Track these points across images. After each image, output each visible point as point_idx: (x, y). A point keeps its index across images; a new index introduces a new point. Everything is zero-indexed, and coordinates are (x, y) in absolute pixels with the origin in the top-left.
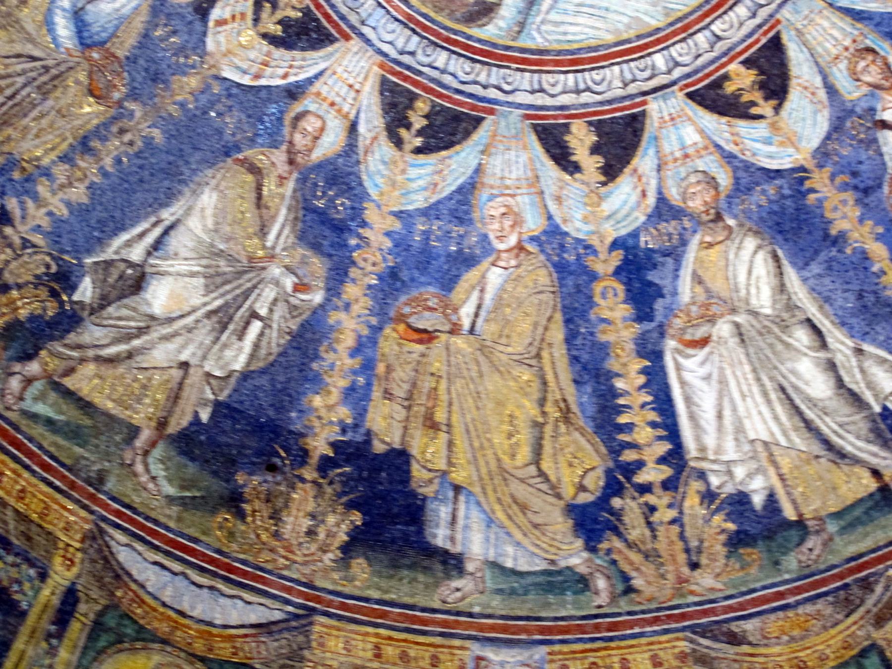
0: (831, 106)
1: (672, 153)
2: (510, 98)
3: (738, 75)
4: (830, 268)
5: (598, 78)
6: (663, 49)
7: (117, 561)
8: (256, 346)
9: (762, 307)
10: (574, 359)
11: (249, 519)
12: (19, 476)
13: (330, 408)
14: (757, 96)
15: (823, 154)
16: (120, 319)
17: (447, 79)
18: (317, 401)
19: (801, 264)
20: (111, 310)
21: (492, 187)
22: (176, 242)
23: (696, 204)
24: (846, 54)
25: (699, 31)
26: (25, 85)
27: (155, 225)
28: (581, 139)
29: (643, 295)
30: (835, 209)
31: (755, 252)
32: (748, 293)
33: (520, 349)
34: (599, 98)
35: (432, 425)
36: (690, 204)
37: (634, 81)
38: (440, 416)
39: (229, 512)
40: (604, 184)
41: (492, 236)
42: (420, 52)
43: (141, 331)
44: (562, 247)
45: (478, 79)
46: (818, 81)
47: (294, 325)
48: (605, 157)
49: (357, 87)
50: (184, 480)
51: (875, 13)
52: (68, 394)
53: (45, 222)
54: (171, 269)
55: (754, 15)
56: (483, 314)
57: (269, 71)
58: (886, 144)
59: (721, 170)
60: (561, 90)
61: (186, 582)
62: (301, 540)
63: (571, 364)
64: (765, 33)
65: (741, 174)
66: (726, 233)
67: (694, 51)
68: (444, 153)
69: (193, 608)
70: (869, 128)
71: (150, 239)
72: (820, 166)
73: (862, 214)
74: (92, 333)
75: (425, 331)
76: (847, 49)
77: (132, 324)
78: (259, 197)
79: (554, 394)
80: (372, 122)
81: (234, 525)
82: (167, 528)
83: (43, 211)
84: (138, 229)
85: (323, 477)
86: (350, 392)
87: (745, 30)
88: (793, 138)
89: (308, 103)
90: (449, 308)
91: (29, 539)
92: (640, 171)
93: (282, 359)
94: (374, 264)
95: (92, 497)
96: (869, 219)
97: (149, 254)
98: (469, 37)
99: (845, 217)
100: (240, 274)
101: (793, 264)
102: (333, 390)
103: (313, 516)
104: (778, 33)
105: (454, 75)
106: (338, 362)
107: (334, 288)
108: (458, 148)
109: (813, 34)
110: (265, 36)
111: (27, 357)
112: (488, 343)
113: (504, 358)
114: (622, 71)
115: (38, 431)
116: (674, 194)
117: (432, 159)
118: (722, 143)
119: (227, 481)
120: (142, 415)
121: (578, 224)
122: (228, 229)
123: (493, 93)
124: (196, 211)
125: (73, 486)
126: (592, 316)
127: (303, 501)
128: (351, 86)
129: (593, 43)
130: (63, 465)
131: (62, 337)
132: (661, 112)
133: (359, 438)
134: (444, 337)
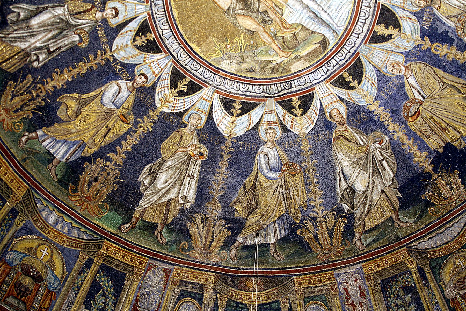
2: (357, 46)
7: (421, 249)
8: (389, 166)
10: (452, 73)
11: (436, 204)
12: (382, 259)
13: (421, 157)
16: (359, 202)
17: (341, 63)
18: (416, 159)
20: (355, 203)
21: (382, 66)
22: (347, 173)
26: (283, 194)
27: (339, 176)
28: (381, 30)
29: (444, 38)
32: (463, 4)
33: (439, 87)
35: (444, 130)
36: (421, 6)
37: (370, 3)
38: (444, 125)
39: (430, 207)
40: (400, 29)
41: (398, 74)
42: (328, 68)
43: (366, 198)
44: (414, 54)
47: (390, 151)
49: (330, 93)
50: (413, 214)
52: (369, 231)
53: (322, 208)
54: (354, 179)
56: (421, 91)
57: (312, 118)
60: (362, 29)
61: (440, 235)
62: (451, 193)
63: (453, 75)
68: (364, 76)
69: (447, 239)
71: (342, 179)
74: (358, 213)
75: (416, 112)
77: (362, 199)
78: (348, 140)
79: (459, 86)
80: (343, 93)
81: (434, 209)
82: (422, 229)
83: (318, 206)
84: (338, 181)
85: (438, 174)
86: (419, 149)
89: (327, 111)
90: (413, 101)
91: (398, 269)
92: (402, 16)
93: (398, 161)
94: (386, 116)
95: (401, 243)
97: (346, 182)
98: (331, 50)
100: (367, 159)
102: (415, 152)
103: (448, 184)
106: (409, 145)
107: (387, 133)
108: (364, 70)
110: (302, 115)
111: (354, 235)
112: (431, 96)
113: (439, 93)
115: (374, 246)
116: (415, 9)
117: (364, 80)
119: (421, 202)
120: (388, 213)
121: (409, 45)
122: (352, 154)
123: (352, 51)
124: (342, 161)
125: (394, 246)
126: (442, 58)
127: (441, 183)
128: (329, 95)
129: (351, 11)
130: (387, 245)
131: (354, 223)
133: (435, 154)
134: (421, 108)
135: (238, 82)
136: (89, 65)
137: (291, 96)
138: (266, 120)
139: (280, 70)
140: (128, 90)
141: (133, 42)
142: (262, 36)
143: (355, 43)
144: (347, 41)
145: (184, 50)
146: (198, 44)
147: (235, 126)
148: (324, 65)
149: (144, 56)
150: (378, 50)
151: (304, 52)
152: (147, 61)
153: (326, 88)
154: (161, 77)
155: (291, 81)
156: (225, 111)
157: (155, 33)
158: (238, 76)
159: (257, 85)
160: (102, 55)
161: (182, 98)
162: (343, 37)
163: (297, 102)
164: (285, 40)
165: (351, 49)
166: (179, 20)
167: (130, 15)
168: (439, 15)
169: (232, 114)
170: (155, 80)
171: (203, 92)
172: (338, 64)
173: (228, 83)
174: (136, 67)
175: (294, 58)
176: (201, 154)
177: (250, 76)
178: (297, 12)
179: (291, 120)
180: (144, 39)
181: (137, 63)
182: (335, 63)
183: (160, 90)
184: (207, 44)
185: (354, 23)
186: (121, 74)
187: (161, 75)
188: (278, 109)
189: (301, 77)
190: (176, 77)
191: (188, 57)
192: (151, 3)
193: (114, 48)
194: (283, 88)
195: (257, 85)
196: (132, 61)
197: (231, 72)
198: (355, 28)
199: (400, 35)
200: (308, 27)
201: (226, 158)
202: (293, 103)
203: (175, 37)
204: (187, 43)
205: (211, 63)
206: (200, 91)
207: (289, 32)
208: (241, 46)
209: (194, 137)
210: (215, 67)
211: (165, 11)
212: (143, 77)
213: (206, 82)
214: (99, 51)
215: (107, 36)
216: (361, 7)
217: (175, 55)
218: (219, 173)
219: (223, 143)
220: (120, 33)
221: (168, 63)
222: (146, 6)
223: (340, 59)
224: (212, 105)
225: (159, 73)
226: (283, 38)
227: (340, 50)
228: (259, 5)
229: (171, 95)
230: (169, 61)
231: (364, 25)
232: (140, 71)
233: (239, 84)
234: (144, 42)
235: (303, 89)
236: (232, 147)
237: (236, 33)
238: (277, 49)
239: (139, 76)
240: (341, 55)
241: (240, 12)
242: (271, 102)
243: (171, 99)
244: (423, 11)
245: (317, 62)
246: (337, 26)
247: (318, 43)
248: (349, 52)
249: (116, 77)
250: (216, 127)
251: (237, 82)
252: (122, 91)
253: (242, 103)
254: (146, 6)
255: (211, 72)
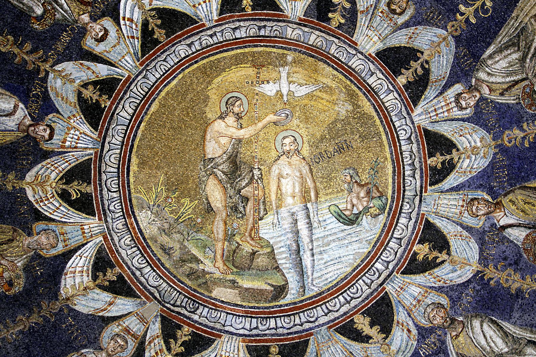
0: (473, 235)
1: (411, 304)
2: (317, 324)
3: (420, 250)
4: (523, 310)
5: (354, 291)
6: (377, 259)
9: (502, 349)
14: (435, 253)
15: (483, 259)
17: (280, 331)
19: (508, 317)
23: (438, 321)
24: (464, 208)
25: (389, 241)
28: (362, 323)
30: (507, 280)
31: (482, 326)
32: (491, 347)
34: (360, 299)
37: (373, 282)
42: (259, 325)
45: (296, 323)
46: (459, 228)
48: (379, 325)
51: (464, 182)
55: (410, 219)
58: (510, 236)
59: (440, 298)
60: (339, 307)
64: (421, 224)
65: (451, 293)
66: (461, 325)
67: (392, 251)
70: (498, 234)
72: (486, 266)
73: (522, 274)
76: (463, 206)
87: (410, 229)
88: (465, 262)
92: (401, 321)
96: (526, 275)
98: (281, 306)
99: (514, 281)
101: (504, 319)
104: (426, 219)
105: (283, 327)
109: (442, 210)
114: (363, 281)
116: (423, 322)
118: (434, 285)
123: (307, 326)
129: (342, 276)
132: (394, 288)
135: (139, 249)
136: (16, 51)
137: (184, 322)
138: (127, 323)
139: (201, 281)
140: (19, 124)
141: (82, 86)
142: (216, 223)
143: (317, 319)
144: (310, 309)
145: (120, 154)
146: (142, 164)
147: (84, 295)
148: (257, 318)
149: (75, 113)
150: (339, 346)
151: (246, 283)
152: (72, 121)
153: (236, 348)
154: (67, 154)
155: (202, 305)
156: (90, 267)
157: (112, 103)
158: (147, 243)
159: (157, 274)
160: (39, 58)
161: (61, 202)
162: (308, 302)
163: (185, 335)
164: (237, 251)
165: (306, 322)
166: (150, 118)
167: (112, 56)
168: (450, 347)
169: (95, 278)
170: (56, 150)
171: (91, 221)
172: (276, 329)
173: (127, 240)
174: (55, 114)
175: (230, 280)
176: (10, 284)
177: (159, 256)
178: (279, 229)
179: (157, 348)
180: (95, 97)
181: (60, 110)
182: (273, 325)
183: (49, 166)
184: (150, 174)
185: (336, 292)
186: (33, 102)
187: (67, 152)
188: (154, 324)
189: (216, 310)
190: (81, 172)
191: (117, 166)
192: (143, 70)
193: (58, 67)
194: (184, 304)
195: (157, 274)
196: (58, 103)
197: (144, 231)
198: (331, 300)
199: (382, 345)
200: (277, 257)
201: (35, 319)
202: (179, 333)
203: (126, 131)
204: (131, 152)
205: (133, 199)
206: (88, 216)
207: (251, 245)
208: (183, 213)
209: (25, 256)
210: (132, 208)
211: (147, 93)
212: (48, 131)
213: (105, 214)
214: (41, 52)
215: (67, 48)
216: (358, 280)
217: (106, 149)
218: (6, 326)
219: (50, 299)
220: (81, 61)
221: (90, 149)
222: (136, 67)
223: (283, 324)
224: (83, 245)
225: (68, 148)
226: (237, 247)
227: (292, 314)
228: (247, 185)
229: (54, 184)
230: (93, 148)
231: (345, 304)
232: (54, 122)
233: (138, 252)
234: (92, 99)
235: (206, 326)
236: (56, 314)
237: (192, 193)
238: (219, 252)
239: (47, 125)
240: (288, 321)
241: (219, 173)
242: (153, 309)
243: (49, 189)
244: (431, 330)
245: (251, 308)
246: (312, 284)
247: (272, 286)
248: (301, 325)
249: (24, 96)
250: (61, 274)
251: (138, 248)
252: (12, 118)
253: (120, 277)
254: (136, 67)
255: (122, 209)
